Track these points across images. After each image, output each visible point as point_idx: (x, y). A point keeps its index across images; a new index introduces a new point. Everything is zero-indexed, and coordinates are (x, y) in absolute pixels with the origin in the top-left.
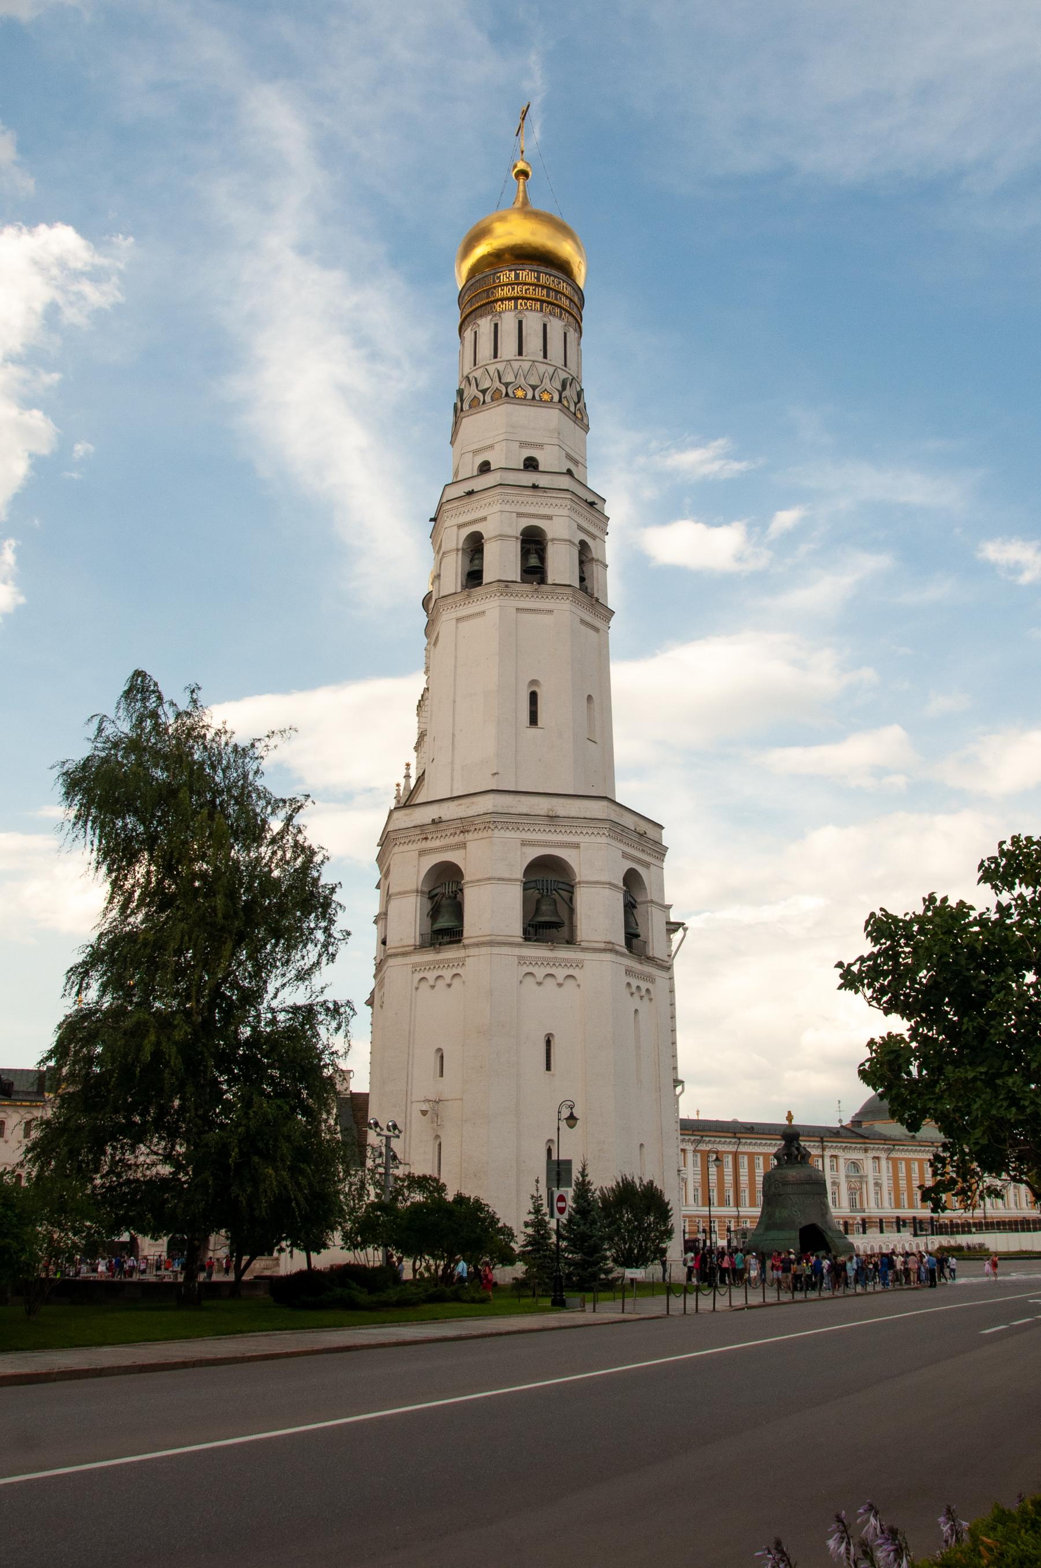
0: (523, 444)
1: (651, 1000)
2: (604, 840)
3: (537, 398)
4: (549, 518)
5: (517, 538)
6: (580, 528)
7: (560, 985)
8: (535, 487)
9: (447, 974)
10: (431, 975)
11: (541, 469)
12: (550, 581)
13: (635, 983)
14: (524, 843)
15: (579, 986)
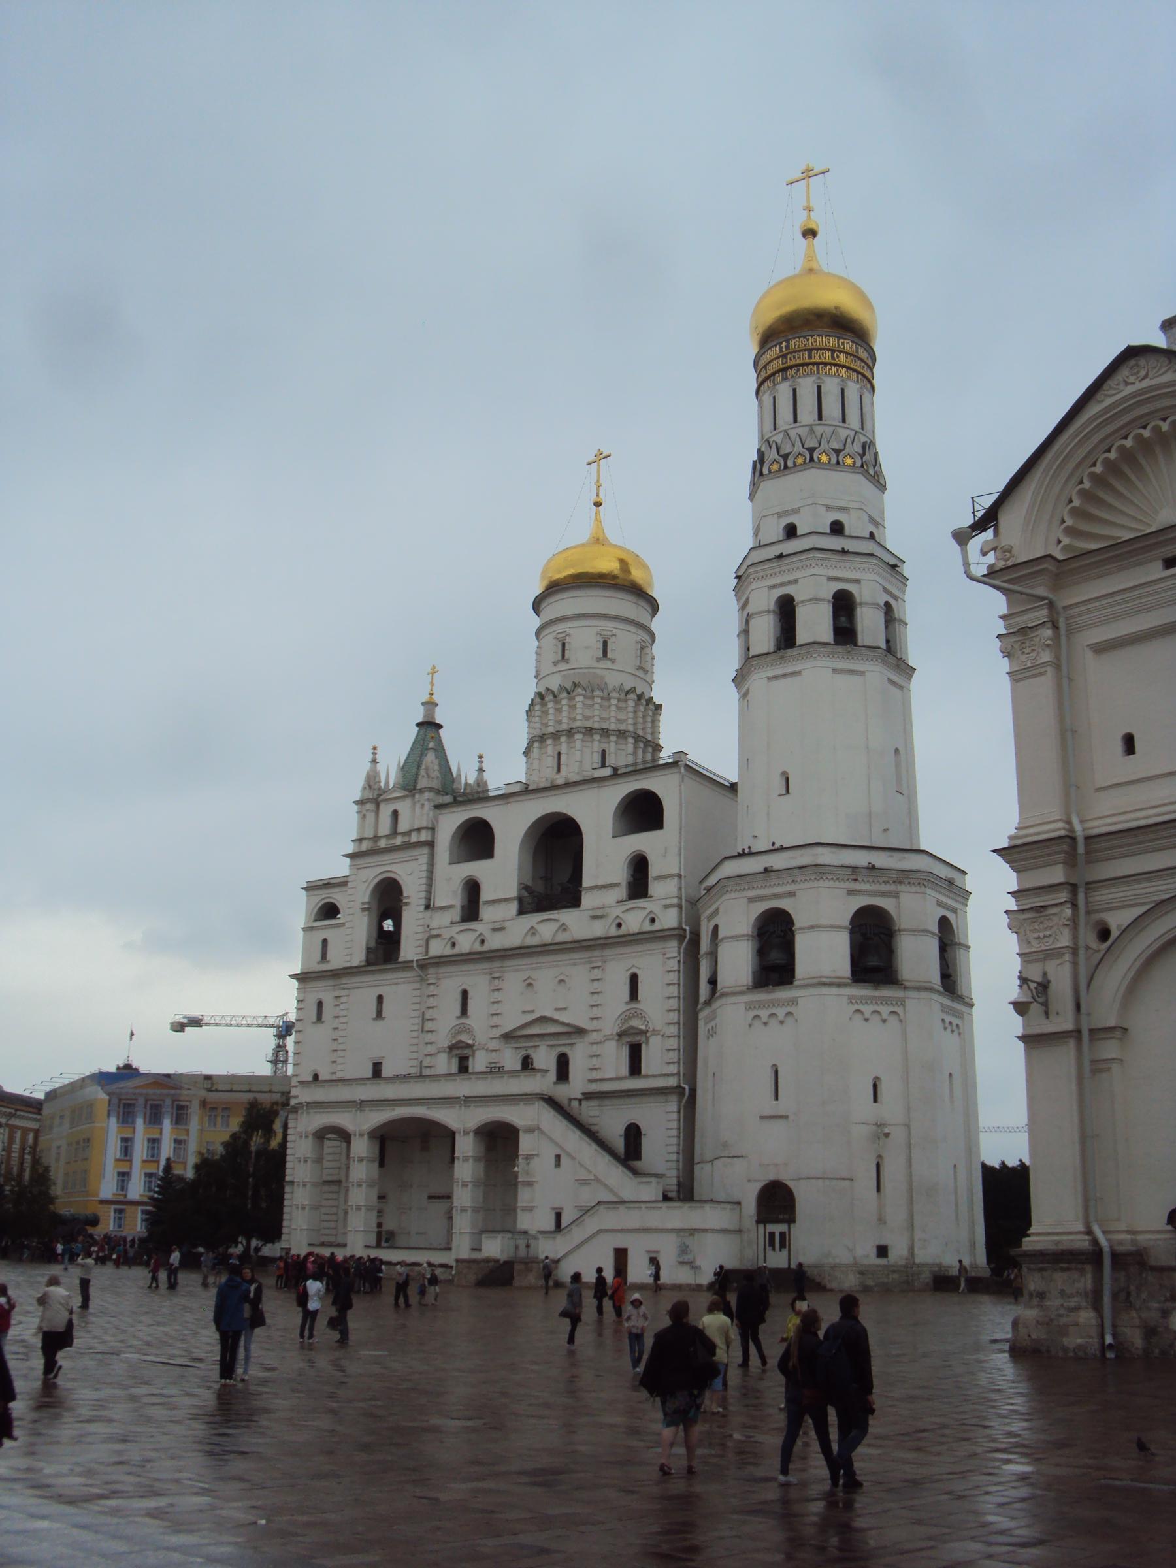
0: (781, 515)
1: (901, 1021)
2: (816, 884)
3: (790, 464)
4: (795, 581)
5: (769, 611)
6: (830, 579)
7: (782, 1022)
8: (781, 556)
9: (713, 1023)
10: (709, 1026)
11: (799, 533)
12: (798, 643)
13: (867, 1009)
14: (752, 900)
15: (797, 1021)
